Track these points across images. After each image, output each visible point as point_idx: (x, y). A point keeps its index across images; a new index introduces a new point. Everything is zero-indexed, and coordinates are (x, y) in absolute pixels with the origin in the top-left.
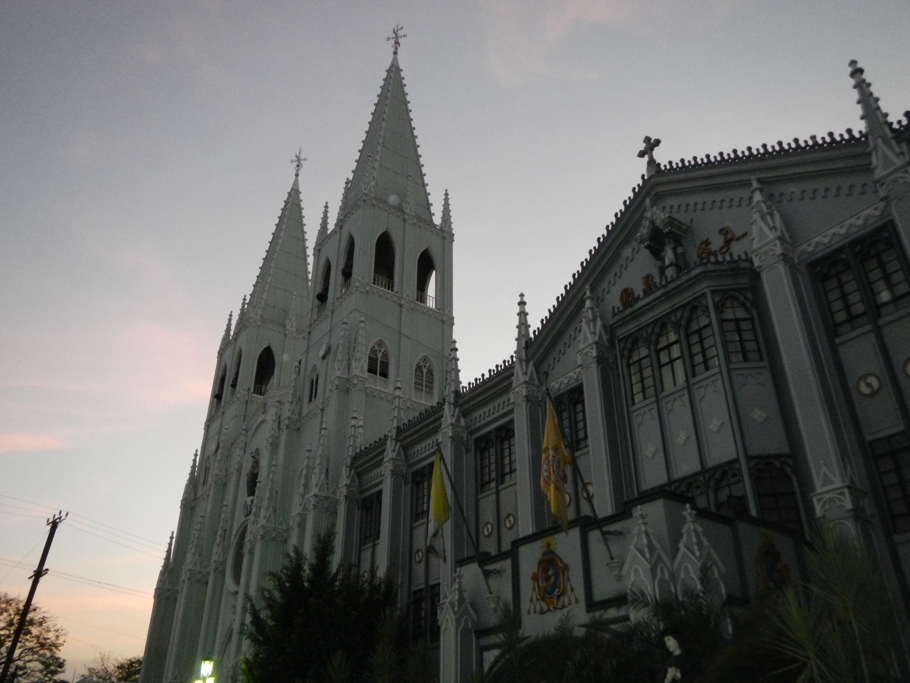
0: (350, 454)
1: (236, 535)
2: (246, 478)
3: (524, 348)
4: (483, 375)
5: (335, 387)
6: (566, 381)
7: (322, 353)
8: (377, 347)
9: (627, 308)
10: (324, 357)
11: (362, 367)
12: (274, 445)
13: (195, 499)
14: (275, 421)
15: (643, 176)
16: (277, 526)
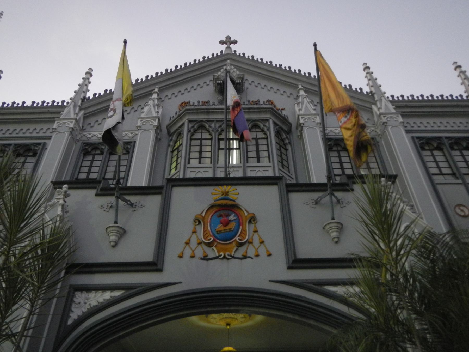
3: (81, 99)
9: (203, 105)
15: (222, 52)
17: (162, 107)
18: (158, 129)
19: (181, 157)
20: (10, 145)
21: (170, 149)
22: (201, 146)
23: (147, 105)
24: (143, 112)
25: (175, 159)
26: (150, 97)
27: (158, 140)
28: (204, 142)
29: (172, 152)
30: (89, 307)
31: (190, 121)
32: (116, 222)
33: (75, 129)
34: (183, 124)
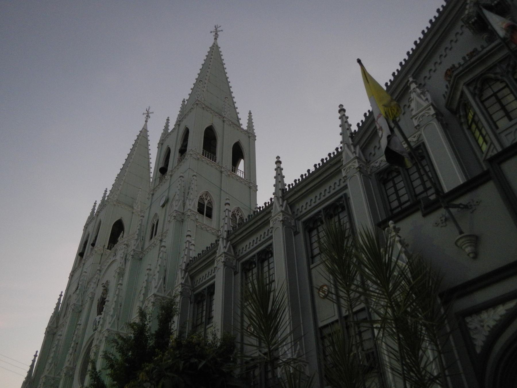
0: (185, 260)
1: (85, 347)
2: (97, 302)
5: (173, 218)
7: (162, 203)
8: (204, 196)
9: (471, 58)
10: (163, 206)
11: (194, 204)
12: (121, 274)
13: (57, 327)
14: (122, 258)
17: (428, 91)
18: (439, 115)
19: (483, 127)
20: (320, 212)
21: (465, 127)
22: (499, 101)
23: (411, 101)
24: (412, 110)
25: (477, 133)
26: (410, 91)
27: (445, 126)
28: (499, 95)
29: (470, 128)
30: (489, 329)
31: (468, 85)
32: (461, 232)
33: (361, 166)
34: (462, 93)
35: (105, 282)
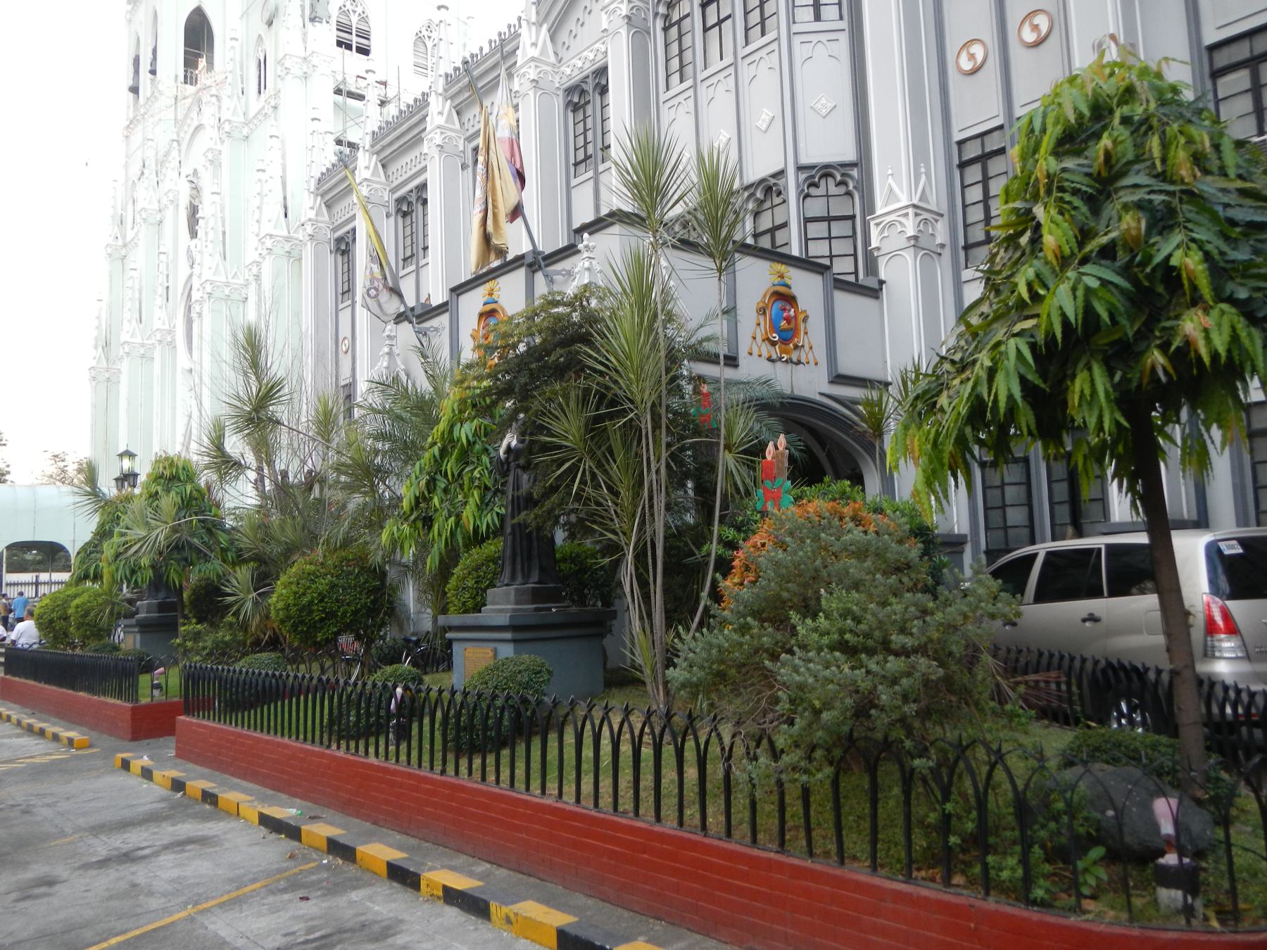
4: (481, 49)
6: (591, 56)
13: (125, 245)
16: (230, 280)
35: (191, 172)
